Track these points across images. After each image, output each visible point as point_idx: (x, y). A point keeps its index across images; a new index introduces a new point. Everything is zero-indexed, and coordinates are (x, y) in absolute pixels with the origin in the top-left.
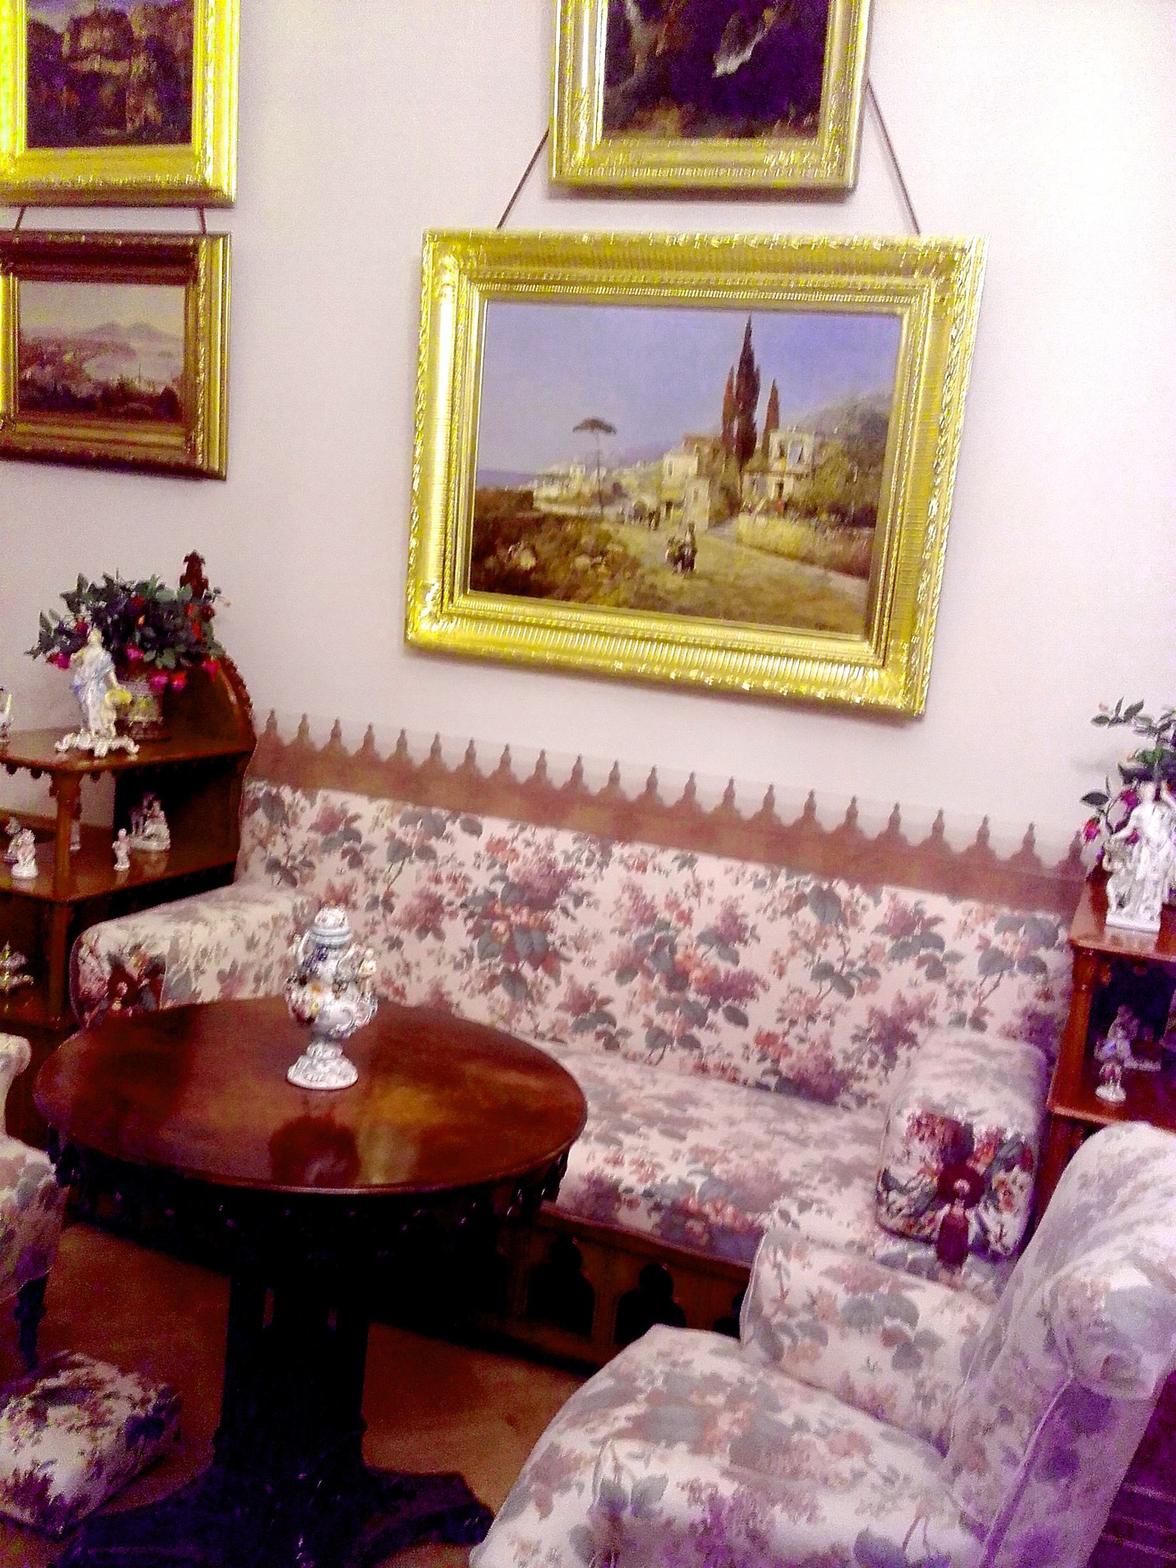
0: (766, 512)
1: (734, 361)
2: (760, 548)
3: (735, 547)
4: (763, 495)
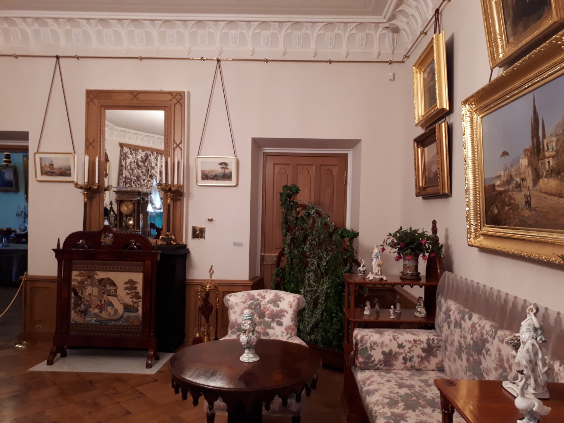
0: (546, 177)
1: (532, 114)
2: (546, 193)
3: (540, 194)
4: (545, 168)
